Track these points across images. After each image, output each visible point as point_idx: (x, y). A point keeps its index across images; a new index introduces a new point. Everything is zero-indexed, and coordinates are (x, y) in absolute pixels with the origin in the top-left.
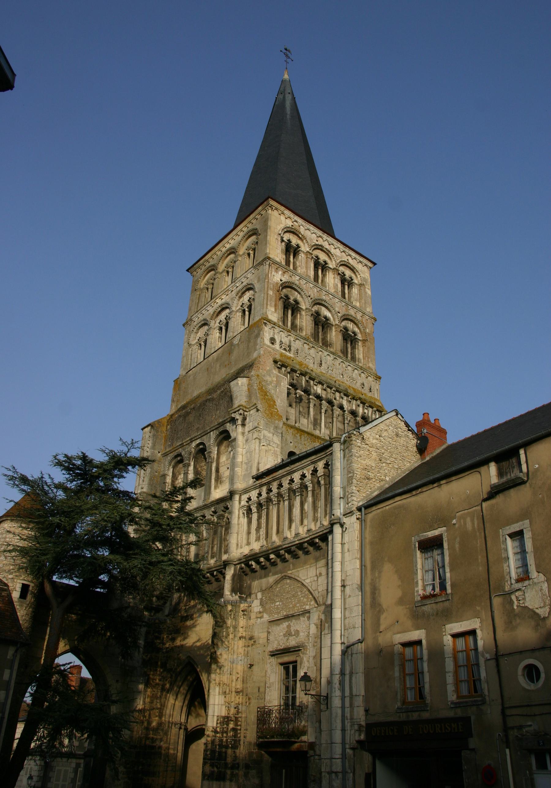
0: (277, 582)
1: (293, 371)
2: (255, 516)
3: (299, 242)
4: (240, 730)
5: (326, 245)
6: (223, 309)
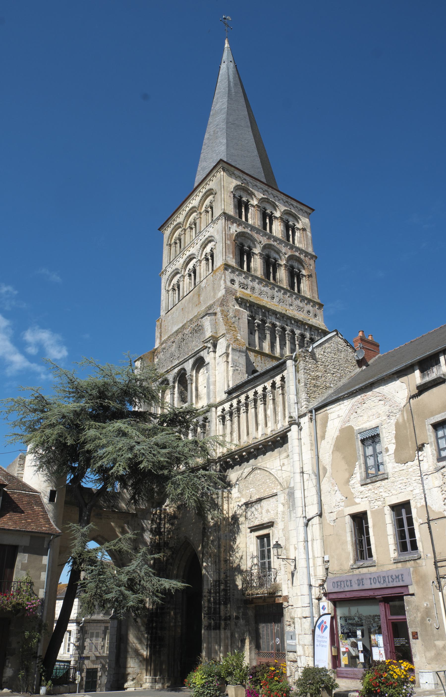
0: (250, 473)
2: (228, 423)
4: (229, 590)
6: (191, 260)
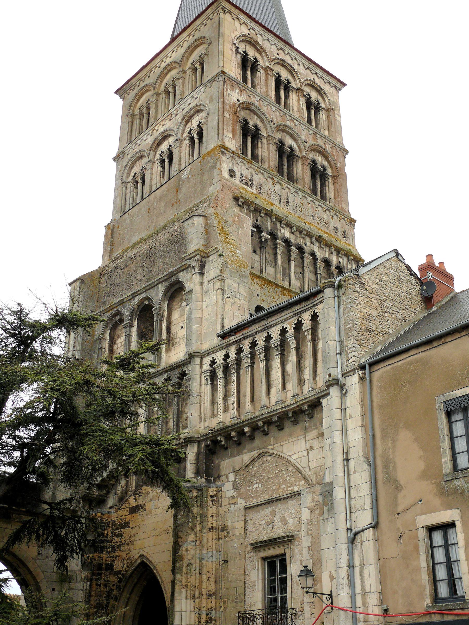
0: (254, 461)
1: (257, 210)
2: (221, 383)
3: (257, 55)
5: (288, 59)
6: (165, 138)
